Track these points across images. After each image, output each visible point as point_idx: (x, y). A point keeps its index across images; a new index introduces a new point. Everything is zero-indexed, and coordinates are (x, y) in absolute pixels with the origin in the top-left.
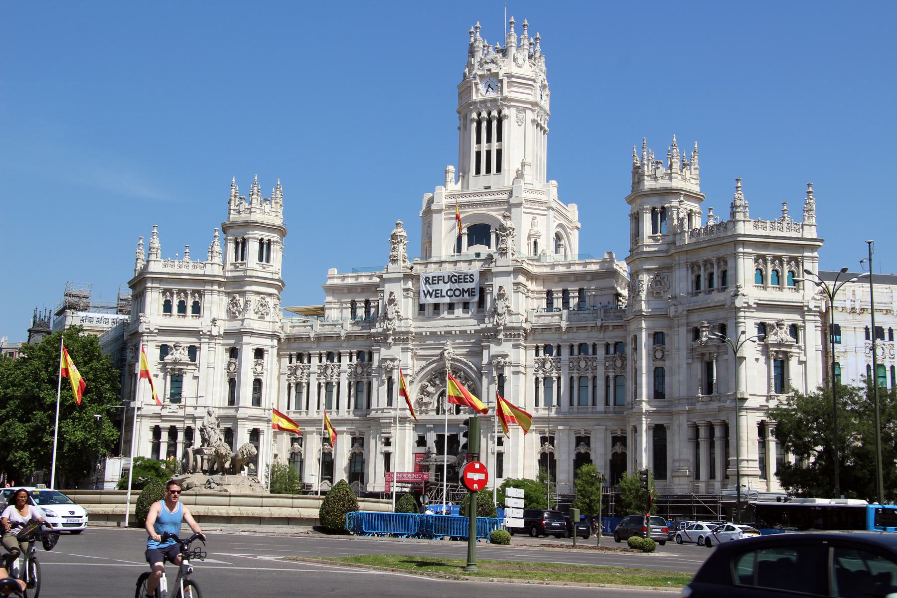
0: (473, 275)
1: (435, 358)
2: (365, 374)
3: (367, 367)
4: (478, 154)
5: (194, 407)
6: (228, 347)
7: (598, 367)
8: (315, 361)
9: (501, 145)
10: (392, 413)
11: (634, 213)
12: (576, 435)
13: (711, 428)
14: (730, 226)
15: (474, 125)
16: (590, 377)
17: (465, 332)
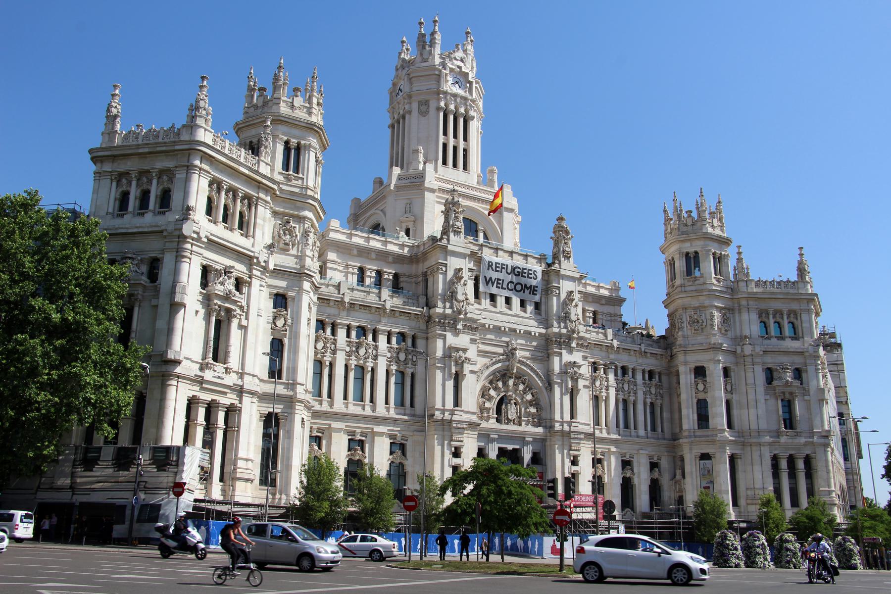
0: (536, 271)
1: (501, 357)
2: (410, 364)
3: (412, 354)
4: (445, 146)
5: (237, 373)
6: (275, 291)
7: (638, 391)
8: (341, 333)
9: (468, 145)
10: (465, 417)
11: (687, 254)
12: (651, 461)
13: (791, 460)
14: (801, 285)
15: (442, 114)
16: (632, 400)
17: (530, 333)
